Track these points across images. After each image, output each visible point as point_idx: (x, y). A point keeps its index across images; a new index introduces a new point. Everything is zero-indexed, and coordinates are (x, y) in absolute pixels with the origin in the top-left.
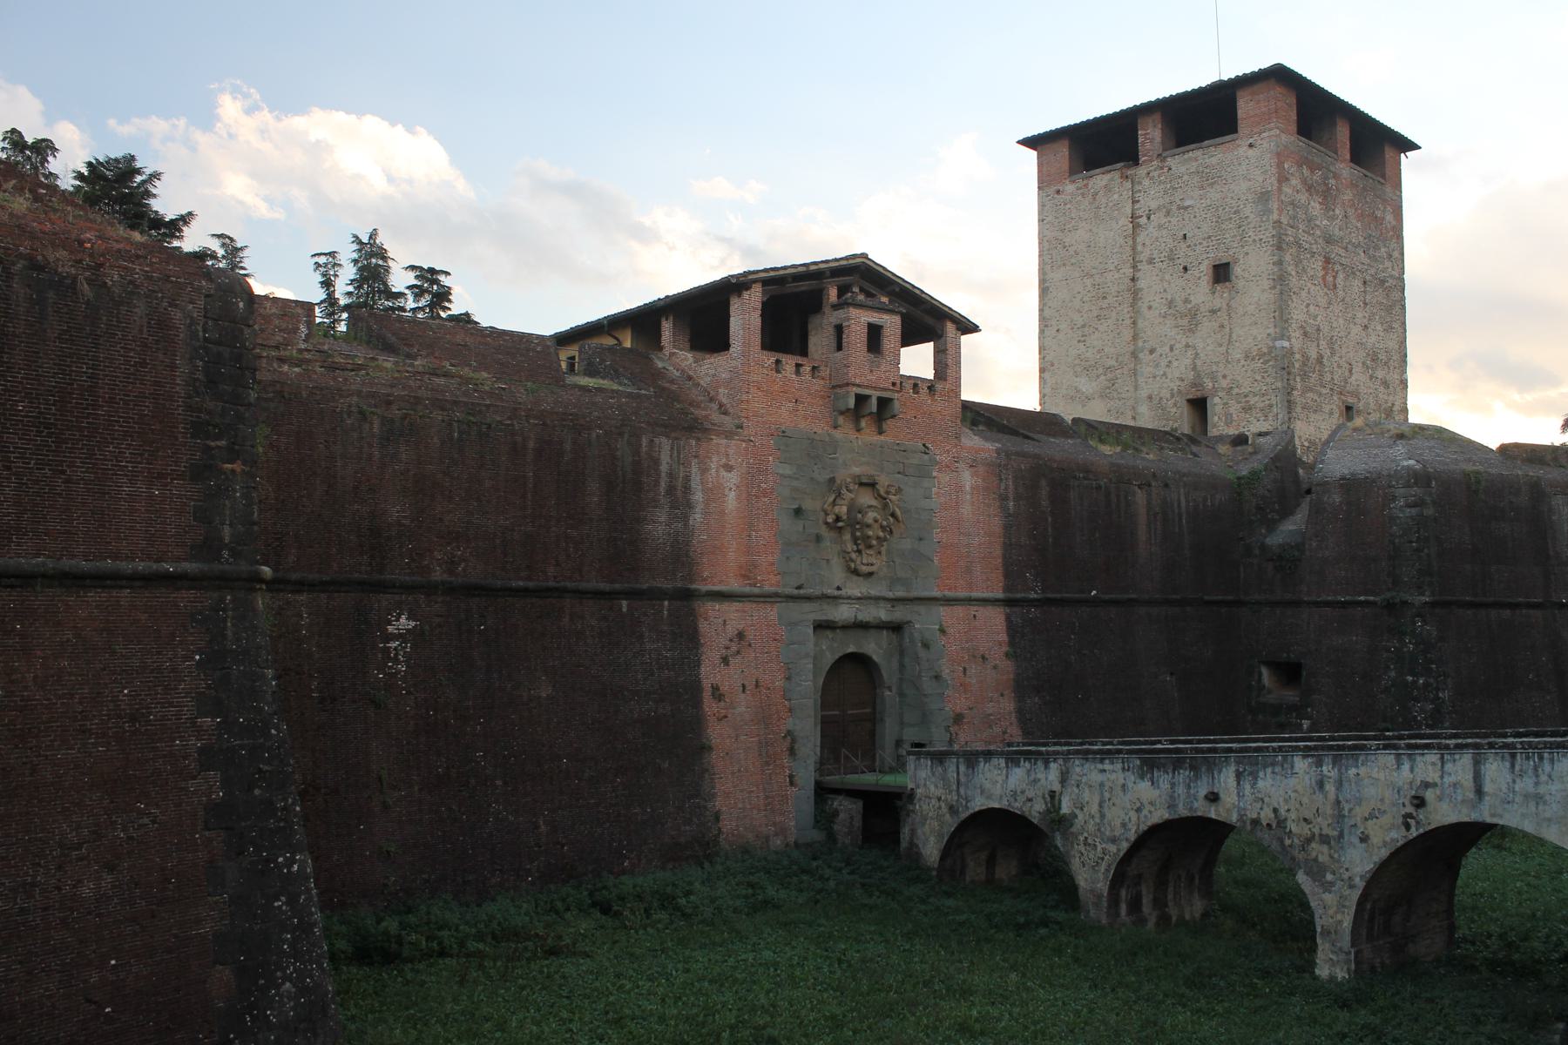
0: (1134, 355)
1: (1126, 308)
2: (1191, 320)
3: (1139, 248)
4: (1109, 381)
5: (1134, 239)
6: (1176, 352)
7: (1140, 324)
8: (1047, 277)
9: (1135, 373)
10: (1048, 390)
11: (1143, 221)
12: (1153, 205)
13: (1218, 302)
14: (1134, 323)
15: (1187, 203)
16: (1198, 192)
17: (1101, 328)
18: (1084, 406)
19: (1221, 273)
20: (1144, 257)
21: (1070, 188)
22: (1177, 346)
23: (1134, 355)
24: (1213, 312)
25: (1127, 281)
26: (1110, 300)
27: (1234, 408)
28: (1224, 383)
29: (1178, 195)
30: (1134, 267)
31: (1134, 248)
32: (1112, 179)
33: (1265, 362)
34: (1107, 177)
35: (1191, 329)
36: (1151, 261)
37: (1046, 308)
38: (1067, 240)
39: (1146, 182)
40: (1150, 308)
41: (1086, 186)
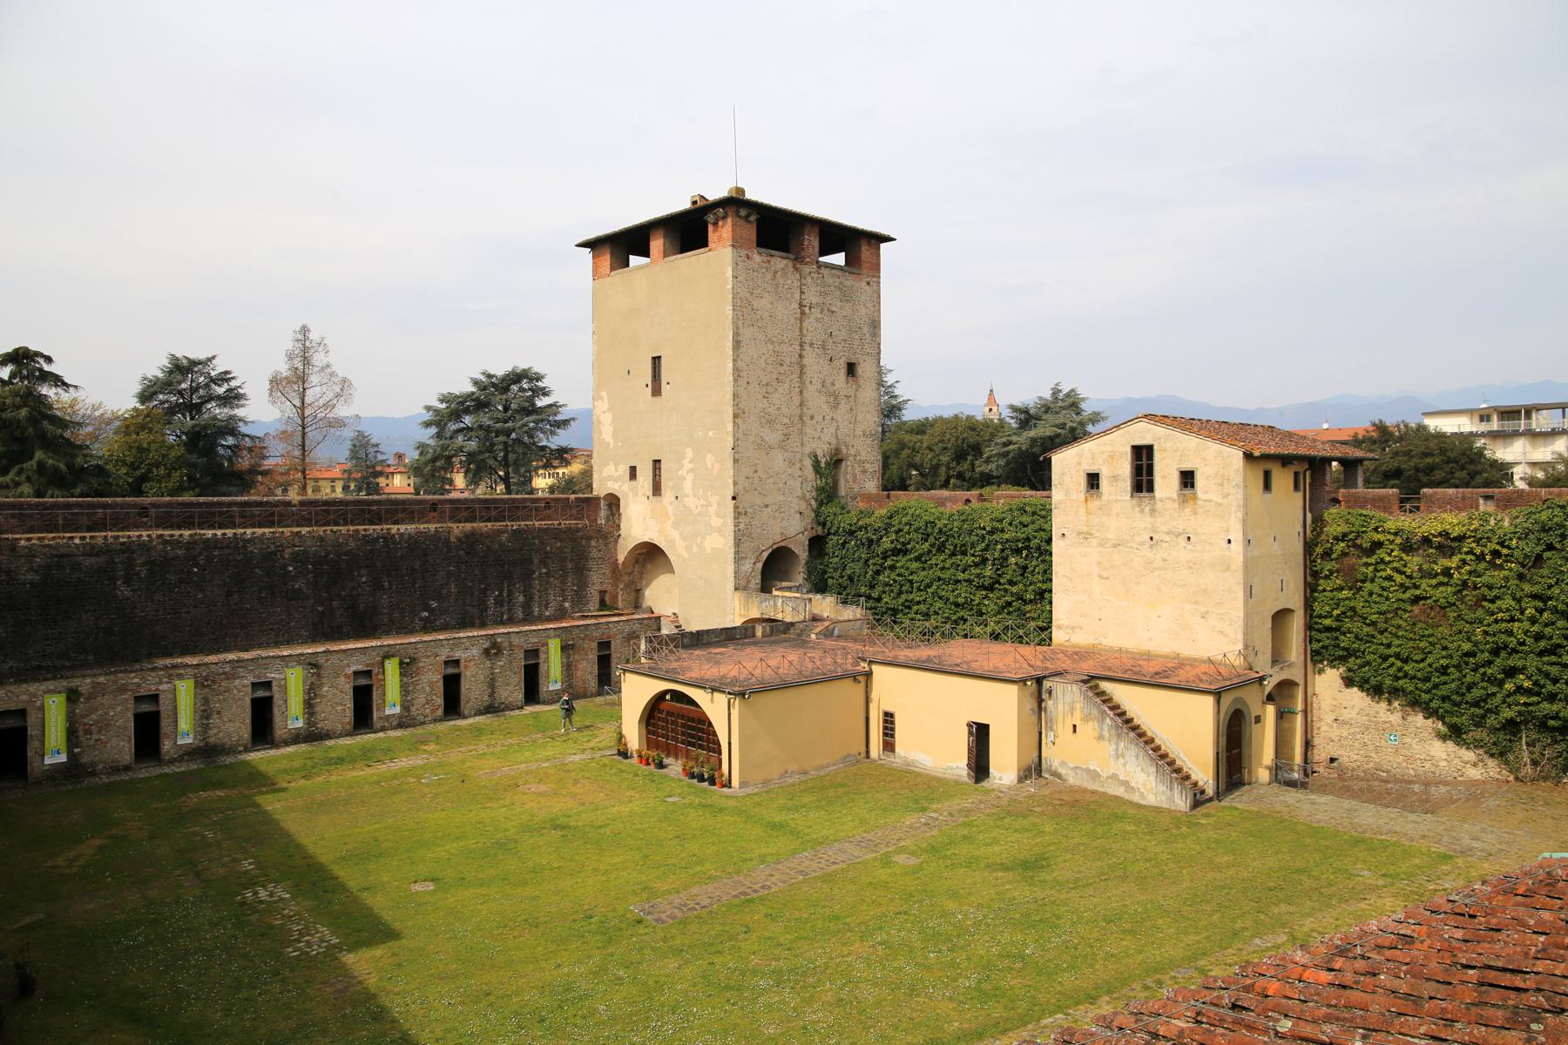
0: (801, 417)
1: (795, 377)
2: (834, 399)
3: (805, 331)
4: (785, 435)
5: (801, 324)
6: (827, 422)
7: (805, 395)
8: (741, 331)
9: (801, 432)
10: (740, 435)
11: (807, 310)
12: (814, 300)
13: (851, 392)
14: (801, 392)
15: (833, 309)
16: (839, 304)
17: (781, 390)
18: (767, 454)
19: (851, 369)
20: (807, 339)
21: (757, 258)
22: (827, 417)
23: (801, 417)
24: (847, 397)
25: (797, 356)
26: (785, 368)
27: (858, 470)
28: (852, 451)
29: (828, 300)
30: (801, 346)
31: (801, 330)
32: (786, 265)
33: (873, 441)
34: (785, 262)
35: (835, 407)
36: (811, 345)
37: (739, 360)
38: (755, 303)
39: (809, 279)
40: (811, 382)
41: (769, 261)
